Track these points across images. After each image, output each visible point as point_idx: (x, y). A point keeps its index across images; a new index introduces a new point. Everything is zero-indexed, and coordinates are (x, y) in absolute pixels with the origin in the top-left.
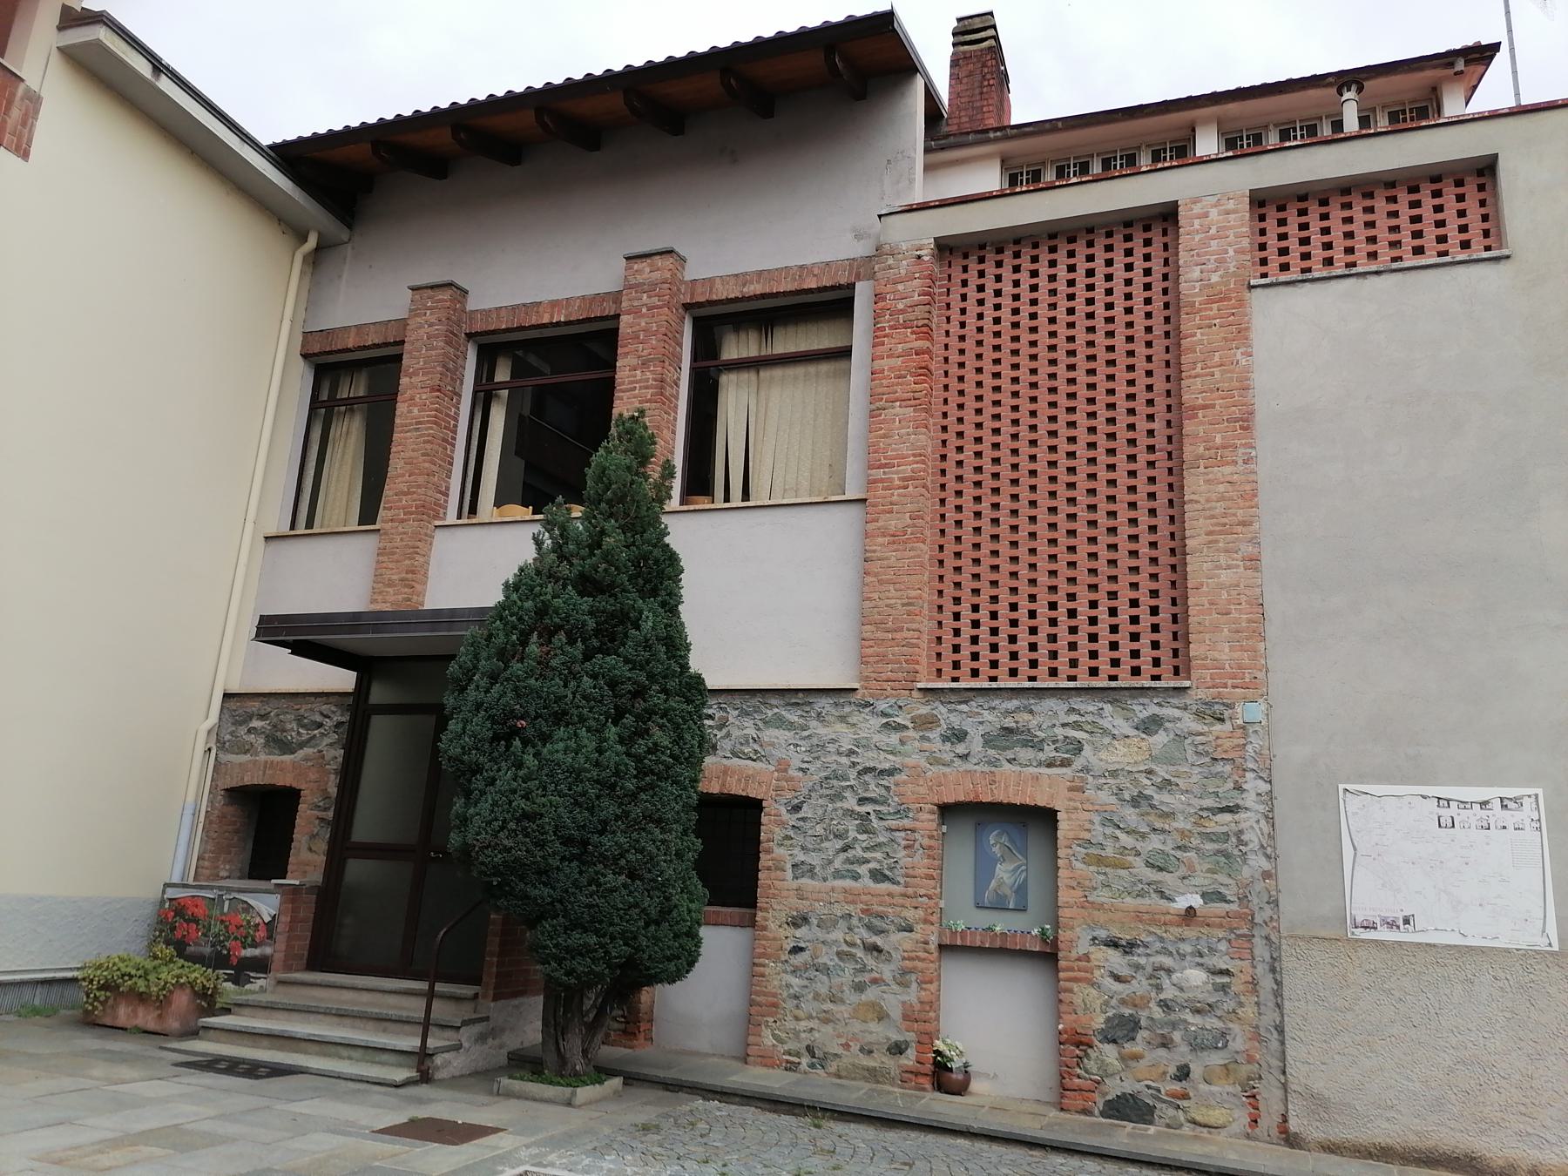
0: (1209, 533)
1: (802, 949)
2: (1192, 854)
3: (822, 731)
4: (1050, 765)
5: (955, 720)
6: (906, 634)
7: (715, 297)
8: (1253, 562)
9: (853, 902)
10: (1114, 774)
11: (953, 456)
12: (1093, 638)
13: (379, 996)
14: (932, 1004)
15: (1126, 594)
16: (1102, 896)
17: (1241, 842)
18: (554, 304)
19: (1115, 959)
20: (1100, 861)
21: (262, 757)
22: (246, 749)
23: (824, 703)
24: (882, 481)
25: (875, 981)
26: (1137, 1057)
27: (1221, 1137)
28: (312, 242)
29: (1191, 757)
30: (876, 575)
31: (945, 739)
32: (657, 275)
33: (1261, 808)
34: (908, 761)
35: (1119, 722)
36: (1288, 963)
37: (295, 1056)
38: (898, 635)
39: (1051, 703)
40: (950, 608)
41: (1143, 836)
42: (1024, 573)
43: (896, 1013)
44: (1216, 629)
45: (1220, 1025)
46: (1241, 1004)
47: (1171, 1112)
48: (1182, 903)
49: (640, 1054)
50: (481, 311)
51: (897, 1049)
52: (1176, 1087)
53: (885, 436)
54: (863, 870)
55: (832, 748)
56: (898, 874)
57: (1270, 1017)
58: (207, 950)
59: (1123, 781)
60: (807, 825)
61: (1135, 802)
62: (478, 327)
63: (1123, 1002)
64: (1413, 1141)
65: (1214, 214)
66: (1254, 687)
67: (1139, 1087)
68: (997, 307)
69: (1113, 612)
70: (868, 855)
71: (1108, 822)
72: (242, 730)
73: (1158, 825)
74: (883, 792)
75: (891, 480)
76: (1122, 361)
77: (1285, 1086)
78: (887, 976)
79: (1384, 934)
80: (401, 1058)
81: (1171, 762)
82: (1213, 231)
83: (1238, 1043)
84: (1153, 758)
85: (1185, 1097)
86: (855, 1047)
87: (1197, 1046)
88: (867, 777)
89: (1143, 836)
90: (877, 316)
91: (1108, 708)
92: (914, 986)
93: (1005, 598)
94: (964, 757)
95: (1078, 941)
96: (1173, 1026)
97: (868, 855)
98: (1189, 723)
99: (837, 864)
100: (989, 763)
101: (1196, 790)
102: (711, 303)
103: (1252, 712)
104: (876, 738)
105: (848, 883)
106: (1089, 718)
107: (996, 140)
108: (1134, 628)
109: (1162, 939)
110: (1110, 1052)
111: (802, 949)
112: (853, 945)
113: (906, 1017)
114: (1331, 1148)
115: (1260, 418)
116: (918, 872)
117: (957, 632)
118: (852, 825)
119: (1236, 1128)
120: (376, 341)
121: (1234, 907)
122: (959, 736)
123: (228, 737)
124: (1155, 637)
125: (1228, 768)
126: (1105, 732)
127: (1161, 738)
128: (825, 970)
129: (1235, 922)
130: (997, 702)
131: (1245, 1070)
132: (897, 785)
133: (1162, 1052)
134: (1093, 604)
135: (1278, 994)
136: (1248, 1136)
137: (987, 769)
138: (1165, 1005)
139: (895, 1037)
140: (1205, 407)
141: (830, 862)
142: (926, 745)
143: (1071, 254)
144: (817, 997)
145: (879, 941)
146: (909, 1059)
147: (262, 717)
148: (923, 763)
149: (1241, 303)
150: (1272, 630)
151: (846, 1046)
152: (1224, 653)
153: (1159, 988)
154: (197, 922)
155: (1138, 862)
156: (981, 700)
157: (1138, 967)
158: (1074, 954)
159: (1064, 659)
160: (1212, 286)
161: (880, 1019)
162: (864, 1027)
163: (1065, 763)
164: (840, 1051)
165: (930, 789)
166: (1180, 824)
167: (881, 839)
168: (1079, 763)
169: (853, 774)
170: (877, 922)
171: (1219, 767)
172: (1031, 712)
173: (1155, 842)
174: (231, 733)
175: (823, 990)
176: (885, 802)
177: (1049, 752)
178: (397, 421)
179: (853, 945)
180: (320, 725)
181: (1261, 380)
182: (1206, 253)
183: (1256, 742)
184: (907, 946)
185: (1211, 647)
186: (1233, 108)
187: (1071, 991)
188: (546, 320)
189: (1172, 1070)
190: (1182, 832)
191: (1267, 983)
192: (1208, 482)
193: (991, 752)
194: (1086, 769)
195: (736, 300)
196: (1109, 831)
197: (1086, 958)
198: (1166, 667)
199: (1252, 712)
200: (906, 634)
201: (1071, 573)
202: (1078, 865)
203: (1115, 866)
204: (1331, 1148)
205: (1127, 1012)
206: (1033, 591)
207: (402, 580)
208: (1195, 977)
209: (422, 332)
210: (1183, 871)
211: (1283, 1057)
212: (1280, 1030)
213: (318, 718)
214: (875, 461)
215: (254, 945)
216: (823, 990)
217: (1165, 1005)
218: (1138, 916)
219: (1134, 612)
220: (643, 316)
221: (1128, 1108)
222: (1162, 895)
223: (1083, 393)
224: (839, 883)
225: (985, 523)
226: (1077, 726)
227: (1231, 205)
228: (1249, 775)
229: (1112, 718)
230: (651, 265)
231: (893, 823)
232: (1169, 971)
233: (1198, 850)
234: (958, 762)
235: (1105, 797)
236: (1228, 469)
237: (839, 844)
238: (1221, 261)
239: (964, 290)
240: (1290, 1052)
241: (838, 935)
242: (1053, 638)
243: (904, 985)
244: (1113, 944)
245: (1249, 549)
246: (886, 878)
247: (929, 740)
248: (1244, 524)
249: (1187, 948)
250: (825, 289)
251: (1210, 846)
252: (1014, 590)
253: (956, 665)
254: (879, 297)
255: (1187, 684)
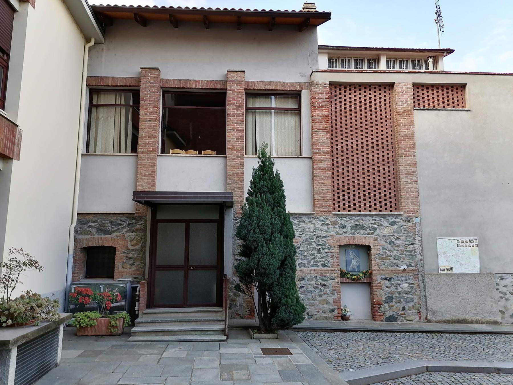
0: (405, 174)
1: (303, 287)
2: (404, 256)
3: (305, 226)
4: (368, 234)
5: (343, 222)
6: (327, 198)
7: (256, 88)
8: (416, 182)
9: (317, 273)
10: (385, 236)
11: (335, 147)
12: (375, 200)
13: (186, 314)
14: (339, 298)
15: (383, 189)
16: (383, 267)
17: (415, 252)
18: (196, 81)
19: (387, 283)
20: (382, 258)
21: (97, 236)
22: (86, 233)
23: (305, 218)
24: (318, 153)
25: (325, 294)
26: (393, 306)
27: (413, 322)
28: (93, 43)
29: (403, 232)
30: (318, 181)
31: (340, 227)
32: (239, 79)
33: (419, 244)
34: (330, 234)
35: (385, 223)
36: (427, 280)
37: (179, 336)
38: (325, 198)
39: (368, 218)
40: (336, 191)
41: (392, 252)
42: (356, 181)
43: (331, 302)
44: (408, 199)
45: (411, 296)
46: (416, 291)
47: (401, 318)
48: (402, 268)
49: (305, 324)
50: (167, 80)
51: (332, 311)
52: (402, 312)
53: (318, 140)
54: (319, 264)
55: (308, 230)
56: (329, 265)
57: (423, 293)
58: (95, 305)
59: (387, 238)
60: (303, 252)
61: (390, 243)
62: (166, 85)
63: (389, 293)
64: (454, 318)
65: (404, 87)
66: (417, 214)
67: (393, 313)
68: (345, 104)
69: (380, 193)
70: (320, 260)
71: (384, 248)
72: (85, 227)
73: (396, 249)
74: (324, 242)
75: (321, 153)
76: (380, 125)
77: (427, 309)
78: (328, 292)
79: (446, 272)
80: (217, 333)
81: (398, 233)
82: (404, 92)
83: (416, 300)
84: (394, 232)
85: (405, 314)
86: (321, 312)
87: (407, 302)
88: (319, 239)
89: (392, 252)
90: (312, 104)
91: (382, 219)
92: (336, 294)
93: (352, 188)
94: (346, 232)
95: (377, 278)
96: (401, 297)
97: (320, 260)
98: (402, 223)
99: (312, 263)
100: (352, 234)
101: (405, 240)
102: (254, 89)
103: (417, 220)
104: (321, 227)
105: (315, 268)
106: (378, 222)
107: (330, 49)
108: (385, 198)
109: (397, 277)
110: (386, 305)
111: (303, 287)
112: (318, 285)
113: (334, 302)
114: (437, 322)
115: (417, 145)
116: (335, 264)
117: (339, 198)
118: (315, 252)
119: (416, 320)
120: (122, 84)
121: (414, 268)
122: (344, 227)
123: (79, 229)
124: (390, 200)
125: (412, 234)
126: (382, 225)
127: (395, 227)
128: (311, 292)
129: (414, 272)
130: (354, 217)
131: (418, 306)
132: (327, 240)
133: (399, 304)
134: (375, 191)
135: (424, 288)
136: (419, 322)
137: (352, 235)
138: (399, 293)
139: (332, 308)
140: (404, 140)
141: (310, 262)
142: (335, 229)
143: (365, 92)
144: (309, 299)
145: (325, 283)
146: (336, 313)
147: (94, 222)
148: (335, 234)
149: (412, 114)
150: (421, 199)
151: (318, 312)
152: (410, 205)
153: (397, 289)
154: (89, 296)
155: (391, 258)
156: (350, 217)
157: (392, 284)
158: (377, 282)
159: (368, 205)
160: (404, 108)
161: (327, 304)
162: (323, 306)
163: (372, 234)
164: (316, 313)
165: (337, 241)
166: (401, 248)
167: (324, 255)
168: (376, 233)
169: (314, 237)
170: (324, 278)
171: (410, 234)
172: (363, 220)
173: (395, 253)
174: (80, 228)
175: (310, 297)
176: (324, 245)
177: (368, 231)
178: (141, 117)
179: (318, 285)
180: (121, 225)
181: (416, 134)
182: (403, 99)
183: (418, 227)
184: (333, 284)
185: (407, 203)
186: (391, 53)
187: (376, 291)
188: (194, 86)
189: (401, 308)
190: (402, 251)
191: (422, 286)
192: (405, 160)
193: (353, 231)
194: (378, 235)
195: (263, 90)
196: (384, 251)
197: (380, 283)
198: (393, 209)
199: (417, 220)
200: (327, 198)
201: (369, 182)
202: (377, 260)
203: (386, 260)
204: (437, 322)
205: (390, 295)
206: (359, 187)
207: (150, 174)
208: (406, 285)
209: (147, 85)
210: (402, 260)
211: (426, 302)
212: (425, 296)
213: (120, 222)
214: (313, 146)
215: (117, 302)
216: (310, 297)
217: (399, 293)
218: (392, 271)
219: (385, 193)
220: (236, 92)
221: (392, 319)
222: (397, 266)
223: (370, 133)
224: (312, 268)
225: (345, 167)
226: (375, 224)
227: (408, 86)
228: (417, 236)
229: (383, 222)
230: (237, 75)
231: (327, 251)
232: (399, 285)
233: (405, 254)
234: (344, 234)
235: (383, 242)
236: (410, 157)
237: (312, 257)
238: (407, 101)
239: (336, 98)
240: (428, 301)
241: (313, 282)
242: (364, 200)
243: (333, 294)
244: (386, 279)
245: (415, 179)
246: (326, 266)
247: (336, 228)
248: (414, 172)
249: (403, 279)
250: (292, 90)
251: (408, 253)
252: (354, 186)
253: (339, 207)
254: (312, 97)
255: (402, 213)
